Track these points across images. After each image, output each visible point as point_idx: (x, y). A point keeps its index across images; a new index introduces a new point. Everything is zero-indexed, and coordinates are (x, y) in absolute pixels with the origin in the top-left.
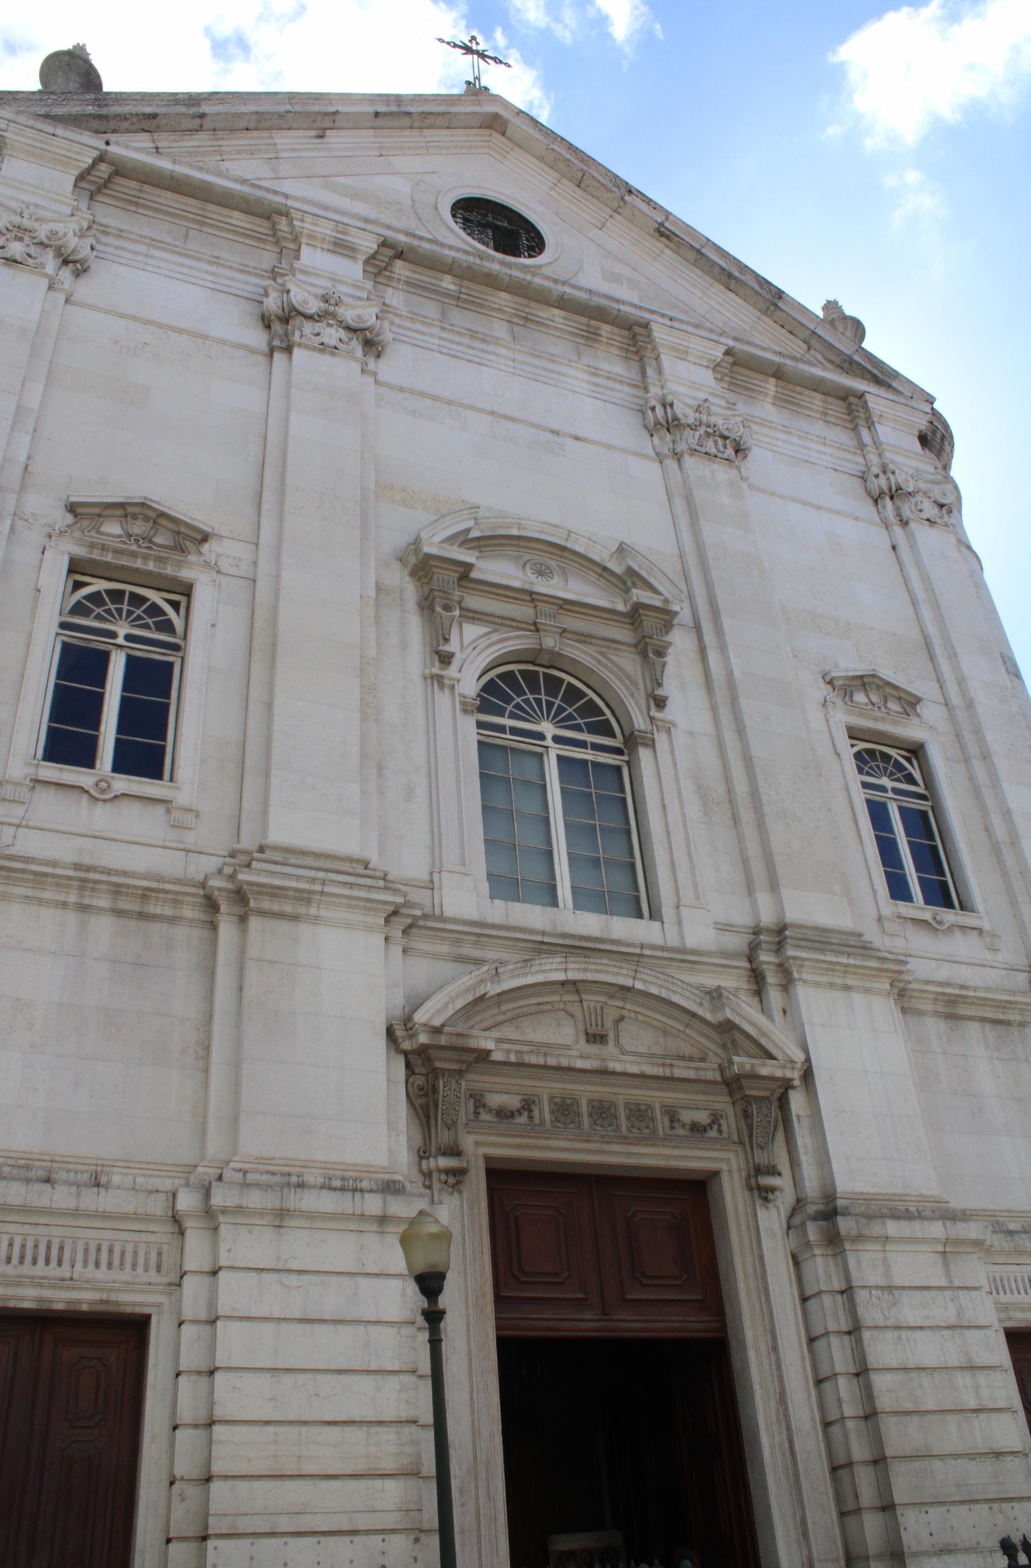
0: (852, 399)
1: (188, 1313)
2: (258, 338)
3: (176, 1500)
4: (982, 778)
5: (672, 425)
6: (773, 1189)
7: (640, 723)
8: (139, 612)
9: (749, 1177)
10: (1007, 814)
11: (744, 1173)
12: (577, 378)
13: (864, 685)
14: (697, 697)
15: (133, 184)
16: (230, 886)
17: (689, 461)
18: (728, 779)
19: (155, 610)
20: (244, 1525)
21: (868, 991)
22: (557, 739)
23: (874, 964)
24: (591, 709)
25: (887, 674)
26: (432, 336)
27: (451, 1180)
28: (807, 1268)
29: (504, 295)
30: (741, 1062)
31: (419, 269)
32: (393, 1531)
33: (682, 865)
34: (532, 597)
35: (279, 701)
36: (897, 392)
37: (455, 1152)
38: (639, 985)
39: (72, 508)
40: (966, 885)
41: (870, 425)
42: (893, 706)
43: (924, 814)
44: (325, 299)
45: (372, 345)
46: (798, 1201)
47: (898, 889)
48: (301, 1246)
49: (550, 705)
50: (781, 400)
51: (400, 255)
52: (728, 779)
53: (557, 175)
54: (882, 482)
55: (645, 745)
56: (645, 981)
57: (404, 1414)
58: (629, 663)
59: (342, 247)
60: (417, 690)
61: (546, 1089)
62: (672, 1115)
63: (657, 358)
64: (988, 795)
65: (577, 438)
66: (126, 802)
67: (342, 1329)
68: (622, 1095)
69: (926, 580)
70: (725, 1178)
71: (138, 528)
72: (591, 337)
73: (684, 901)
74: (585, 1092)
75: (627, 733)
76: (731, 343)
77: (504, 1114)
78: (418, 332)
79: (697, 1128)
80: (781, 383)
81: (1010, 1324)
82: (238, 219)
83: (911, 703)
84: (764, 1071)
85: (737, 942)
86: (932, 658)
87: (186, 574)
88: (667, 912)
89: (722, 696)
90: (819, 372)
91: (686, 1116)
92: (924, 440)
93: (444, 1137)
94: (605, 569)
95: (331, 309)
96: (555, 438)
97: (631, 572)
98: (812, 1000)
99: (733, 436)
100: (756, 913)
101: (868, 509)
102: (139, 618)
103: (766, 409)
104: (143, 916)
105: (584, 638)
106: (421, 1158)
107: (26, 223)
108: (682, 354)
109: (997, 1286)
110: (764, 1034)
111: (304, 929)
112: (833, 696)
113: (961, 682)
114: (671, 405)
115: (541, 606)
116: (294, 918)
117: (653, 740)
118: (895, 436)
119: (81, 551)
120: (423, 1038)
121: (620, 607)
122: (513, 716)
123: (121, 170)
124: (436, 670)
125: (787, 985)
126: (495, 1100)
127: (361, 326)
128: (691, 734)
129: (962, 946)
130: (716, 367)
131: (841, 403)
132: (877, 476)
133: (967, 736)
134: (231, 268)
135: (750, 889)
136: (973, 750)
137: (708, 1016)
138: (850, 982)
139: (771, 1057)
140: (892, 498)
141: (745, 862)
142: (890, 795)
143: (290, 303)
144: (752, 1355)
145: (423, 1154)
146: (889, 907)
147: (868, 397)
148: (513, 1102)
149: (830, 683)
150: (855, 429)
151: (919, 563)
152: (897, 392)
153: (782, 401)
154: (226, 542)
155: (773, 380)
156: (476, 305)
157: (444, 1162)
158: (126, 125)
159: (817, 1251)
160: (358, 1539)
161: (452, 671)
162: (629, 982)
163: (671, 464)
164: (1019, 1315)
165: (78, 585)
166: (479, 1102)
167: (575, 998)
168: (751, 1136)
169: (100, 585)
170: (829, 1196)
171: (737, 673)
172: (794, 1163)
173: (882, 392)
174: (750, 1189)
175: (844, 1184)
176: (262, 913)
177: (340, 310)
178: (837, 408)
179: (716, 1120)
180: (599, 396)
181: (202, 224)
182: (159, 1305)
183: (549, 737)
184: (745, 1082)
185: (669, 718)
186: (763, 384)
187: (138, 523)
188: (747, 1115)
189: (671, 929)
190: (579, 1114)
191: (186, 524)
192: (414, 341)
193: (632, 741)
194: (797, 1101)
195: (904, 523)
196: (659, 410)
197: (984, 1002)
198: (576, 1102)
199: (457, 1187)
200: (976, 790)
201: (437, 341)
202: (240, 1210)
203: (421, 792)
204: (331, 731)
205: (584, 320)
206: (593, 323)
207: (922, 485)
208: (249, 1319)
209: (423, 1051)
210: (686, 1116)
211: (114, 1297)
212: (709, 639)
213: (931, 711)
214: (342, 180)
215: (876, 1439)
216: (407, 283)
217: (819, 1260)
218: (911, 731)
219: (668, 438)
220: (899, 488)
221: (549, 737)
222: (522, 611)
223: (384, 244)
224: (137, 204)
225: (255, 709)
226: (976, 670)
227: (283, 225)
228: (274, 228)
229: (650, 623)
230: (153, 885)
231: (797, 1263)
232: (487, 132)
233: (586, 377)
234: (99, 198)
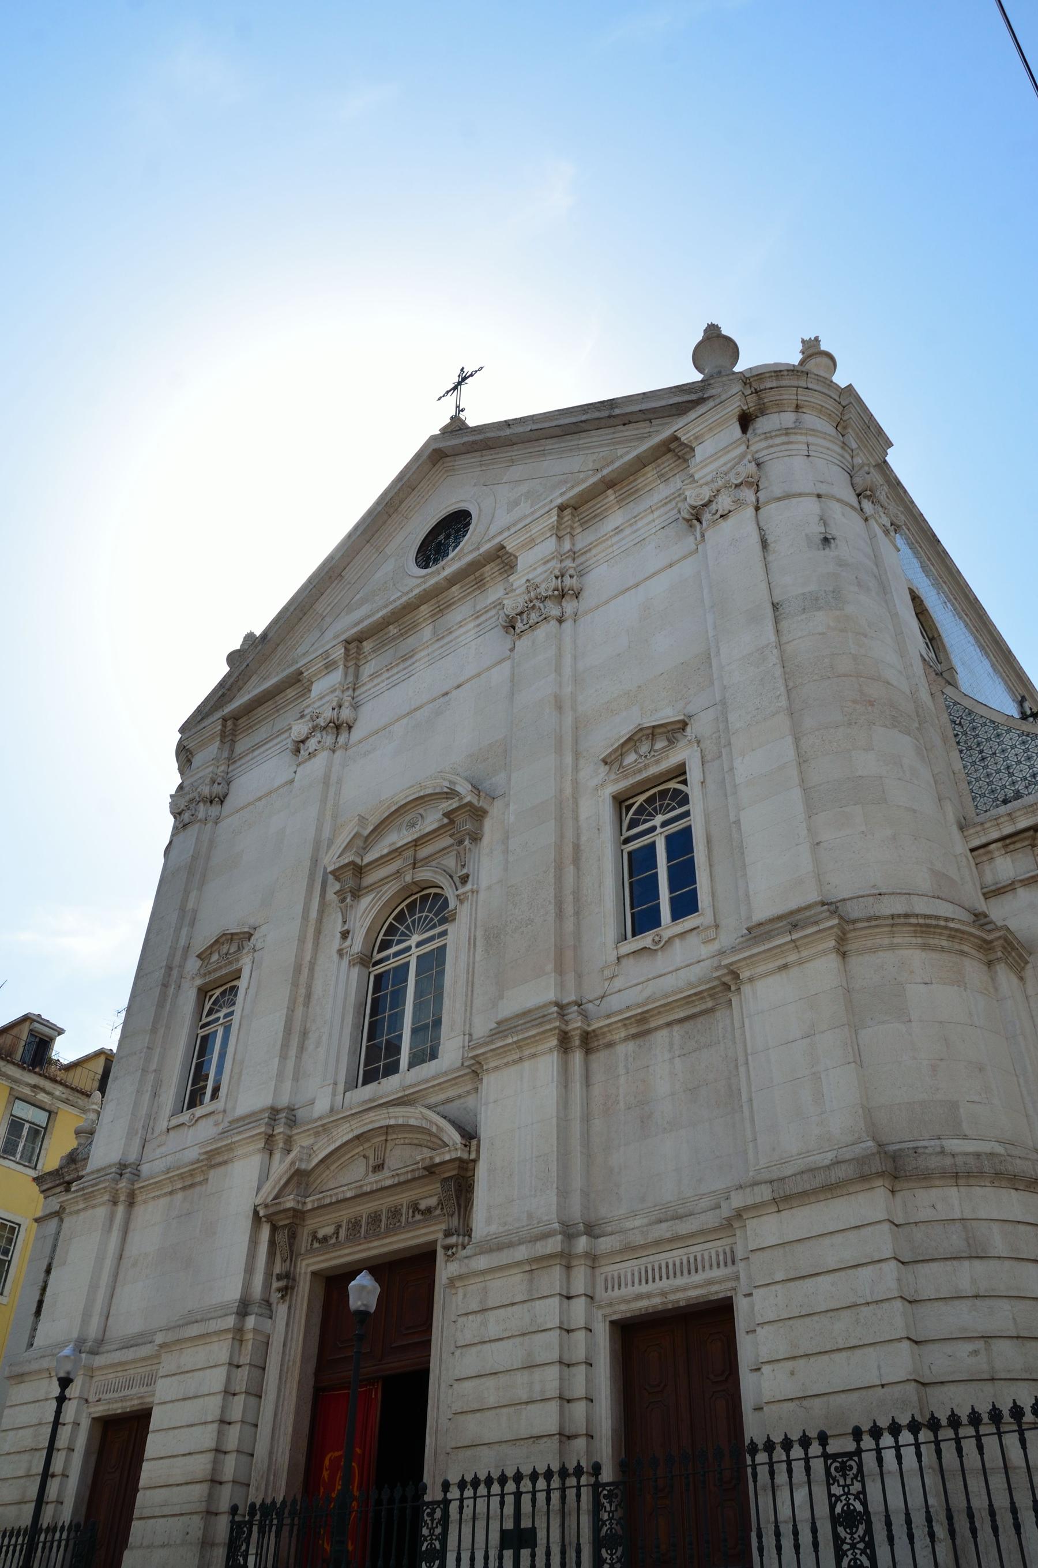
15: (245, 718)
29: (422, 608)
31: (375, 637)
38: (392, 1122)
51: (360, 641)
56: (395, 1117)
62: (415, 1207)
80: (617, 488)
96: (447, 698)
116: (225, 1162)
148: (329, 1230)
153: (621, 501)
154: (263, 928)
155: (610, 492)
158: (240, 683)
169: (218, 992)
178: (667, 462)
186: (606, 501)
197: (668, 1007)
205: (472, 577)
206: (477, 574)
210: (423, 1206)
223: (348, 642)
224: (251, 727)
230: (191, 1167)
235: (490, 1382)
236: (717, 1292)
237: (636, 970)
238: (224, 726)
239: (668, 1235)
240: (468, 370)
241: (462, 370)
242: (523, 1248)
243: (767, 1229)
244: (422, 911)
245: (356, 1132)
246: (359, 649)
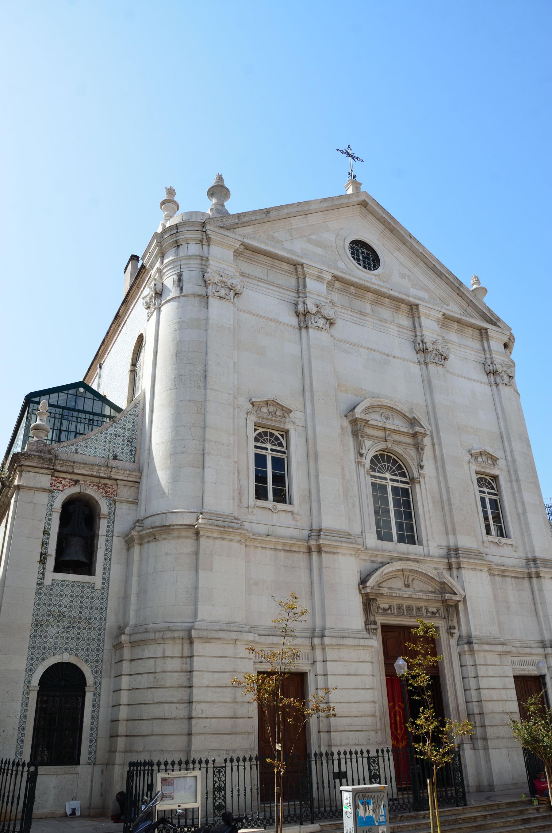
0: (483, 331)
1: (319, 673)
2: (294, 321)
3: (321, 722)
4: (516, 489)
5: (424, 351)
6: (454, 633)
7: (416, 475)
8: (276, 443)
9: (447, 629)
10: (523, 503)
11: (446, 628)
12: (393, 329)
13: (481, 454)
14: (432, 461)
16: (316, 543)
17: (430, 366)
18: (441, 493)
19: (277, 439)
20: (339, 729)
21: (481, 570)
22: (392, 480)
23: (484, 563)
24: (400, 468)
25: (489, 450)
26: (348, 315)
27: (375, 632)
28: (462, 657)
29: (370, 294)
30: (447, 596)
31: (343, 284)
32: (371, 730)
33: (428, 526)
34: (385, 429)
35: (320, 476)
36: (499, 327)
37: (375, 623)
38: (420, 570)
39: (252, 404)
40: (508, 528)
41: (488, 341)
42: (490, 462)
43: (496, 501)
44: (317, 306)
45: (331, 322)
46: (460, 637)
47: (488, 532)
48: (345, 654)
49: (391, 468)
50: (458, 331)
52: (441, 493)
53: (384, 227)
54: (491, 368)
55: (417, 483)
57: (372, 700)
58: (412, 452)
59: (320, 278)
60: (354, 466)
61: (395, 602)
62: (427, 609)
63: (419, 317)
64: (517, 495)
65: (394, 357)
66: (281, 512)
67: (356, 677)
68: (414, 604)
69: (503, 409)
70: (440, 628)
71: (271, 409)
72: (398, 308)
73: (429, 539)
74: (405, 603)
75: (411, 477)
76: (445, 311)
77: (384, 609)
78: (343, 313)
79: (433, 613)
80: (459, 324)
81: (515, 675)
82: (285, 266)
83: (494, 460)
84: (454, 598)
85: (443, 552)
86: (502, 441)
87: (287, 427)
88: (424, 542)
89: (439, 463)
90: (473, 321)
91: (431, 610)
92: (506, 346)
93: (372, 618)
94: (405, 415)
95: (320, 310)
97: (414, 418)
98: (466, 574)
99: (445, 355)
100: (449, 542)
101: (484, 378)
102: (273, 442)
103: (453, 336)
104: (291, 551)
105: (399, 443)
106: (366, 625)
107: (223, 279)
108: (428, 316)
109: (513, 663)
110: (454, 586)
111: (336, 556)
112: (472, 460)
113: (512, 452)
114: (425, 343)
115: (387, 432)
116: (334, 553)
117: (420, 481)
118: (496, 345)
119: (256, 420)
120: (369, 590)
121: (411, 432)
122: (378, 472)
123: (247, 247)
124: (359, 460)
125: (459, 568)
126: (382, 606)
127: (329, 318)
128: (430, 477)
129: (507, 551)
130: (438, 320)
131: (478, 331)
132: (489, 366)
133: (512, 472)
134: (284, 289)
135: (447, 534)
136: (514, 478)
137: (438, 580)
138: (477, 568)
139: (456, 594)
140: (493, 374)
141: (446, 524)
142: (487, 494)
143: (307, 309)
144: (447, 682)
145: (366, 623)
146: (486, 538)
147: (489, 330)
148: (387, 606)
149: (471, 454)
150: (482, 341)
151: (501, 402)
152: (499, 327)
153: (458, 331)
155: (456, 323)
156: (362, 297)
157: (373, 626)
159: (467, 653)
160: (363, 732)
161: (363, 460)
162: (417, 569)
163: (423, 366)
164: (518, 672)
165: (256, 430)
166: (379, 607)
167: (401, 573)
168: (448, 617)
170: (469, 636)
171: (445, 455)
172: (459, 625)
173: (494, 328)
174: (448, 633)
175: (474, 633)
176: (326, 552)
177: (322, 310)
178: (477, 333)
179: (438, 611)
180: (400, 336)
181: (272, 267)
182: (310, 670)
183: (389, 479)
184: (448, 601)
185: (425, 473)
187: (271, 407)
188: (447, 610)
189: (425, 548)
190: (403, 609)
191: (286, 408)
192: (342, 318)
193: (412, 481)
194: (461, 606)
195: (497, 385)
196: (421, 344)
198: (402, 606)
199: (376, 634)
200: (513, 493)
201: (349, 317)
202: (331, 645)
203: (357, 504)
204: (335, 487)
205: (396, 303)
206: (399, 303)
207: (505, 369)
208: (334, 675)
209: (367, 594)
210: (431, 610)
211: (300, 668)
212: (436, 441)
213: (502, 463)
214: (312, 237)
215: (481, 707)
217: (467, 656)
218: (495, 472)
219: (423, 355)
220: (497, 371)
221: (389, 479)
222: (381, 434)
225: (313, 479)
226: (517, 446)
227: (300, 269)
228: (296, 269)
229: (419, 437)
231: (460, 655)
232: (360, 206)
233: (396, 328)
234: (238, 258)
235: (493, 691)
239: (529, 652)
245: (402, 567)
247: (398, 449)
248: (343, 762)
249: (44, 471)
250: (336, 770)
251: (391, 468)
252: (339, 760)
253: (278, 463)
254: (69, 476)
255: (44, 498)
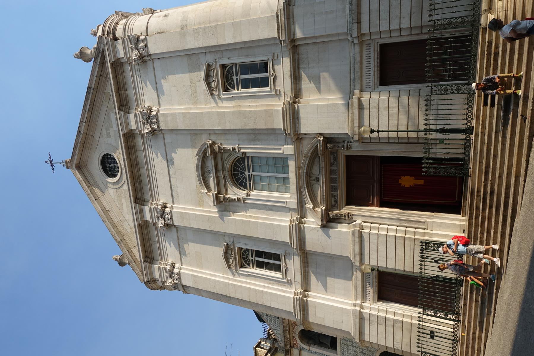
59: (141, 212)
71: (229, 256)
153: (125, 89)
216: (141, 194)
236: (377, 48)
237: (279, 86)
238: (147, 262)
240: (47, 159)
241: (46, 162)
242: (354, 110)
243: (365, 29)
244: (239, 167)
246: (139, 199)
247: (228, 166)
248: (424, 331)
249: (292, 351)
250: (429, 336)
251: (242, 177)
252: (423, 333)
253: (259, 254)
254: (292, 340)
255: (304, 353)
